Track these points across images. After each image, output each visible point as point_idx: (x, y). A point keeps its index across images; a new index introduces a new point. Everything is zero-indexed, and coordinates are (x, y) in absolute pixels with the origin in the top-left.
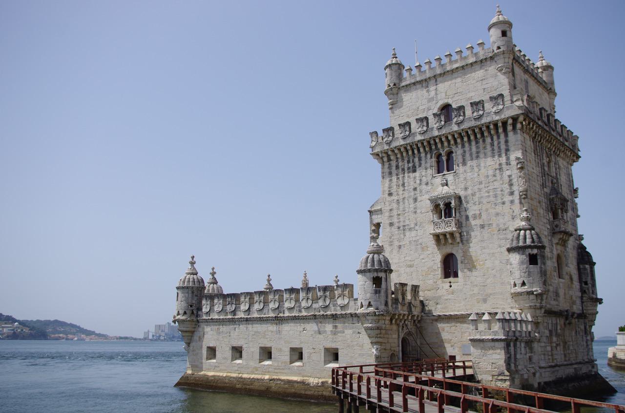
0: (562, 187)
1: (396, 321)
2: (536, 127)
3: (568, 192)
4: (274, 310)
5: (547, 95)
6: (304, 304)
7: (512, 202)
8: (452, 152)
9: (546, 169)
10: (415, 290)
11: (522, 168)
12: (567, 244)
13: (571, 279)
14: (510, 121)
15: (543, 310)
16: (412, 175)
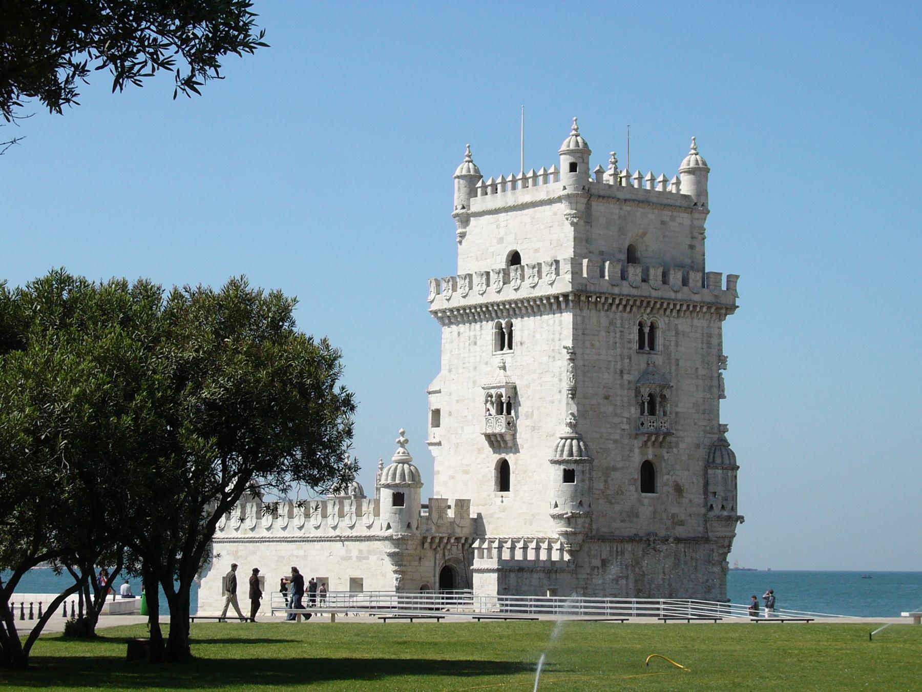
0: (681, 363)
1: (431, 547)
2: (606, 299)
3: (698, 365)
4: (301, 528)
5: (685, 215)
6: (330, 521)
7: (560, 401)
8: (512, 325)
9: (635, 346)
10: (462, 506)
11: (571, 360)
12: (677, 443)
13: (679, 490)
14: (561, 299)
15: (580, 538)
16: (473, 348)
